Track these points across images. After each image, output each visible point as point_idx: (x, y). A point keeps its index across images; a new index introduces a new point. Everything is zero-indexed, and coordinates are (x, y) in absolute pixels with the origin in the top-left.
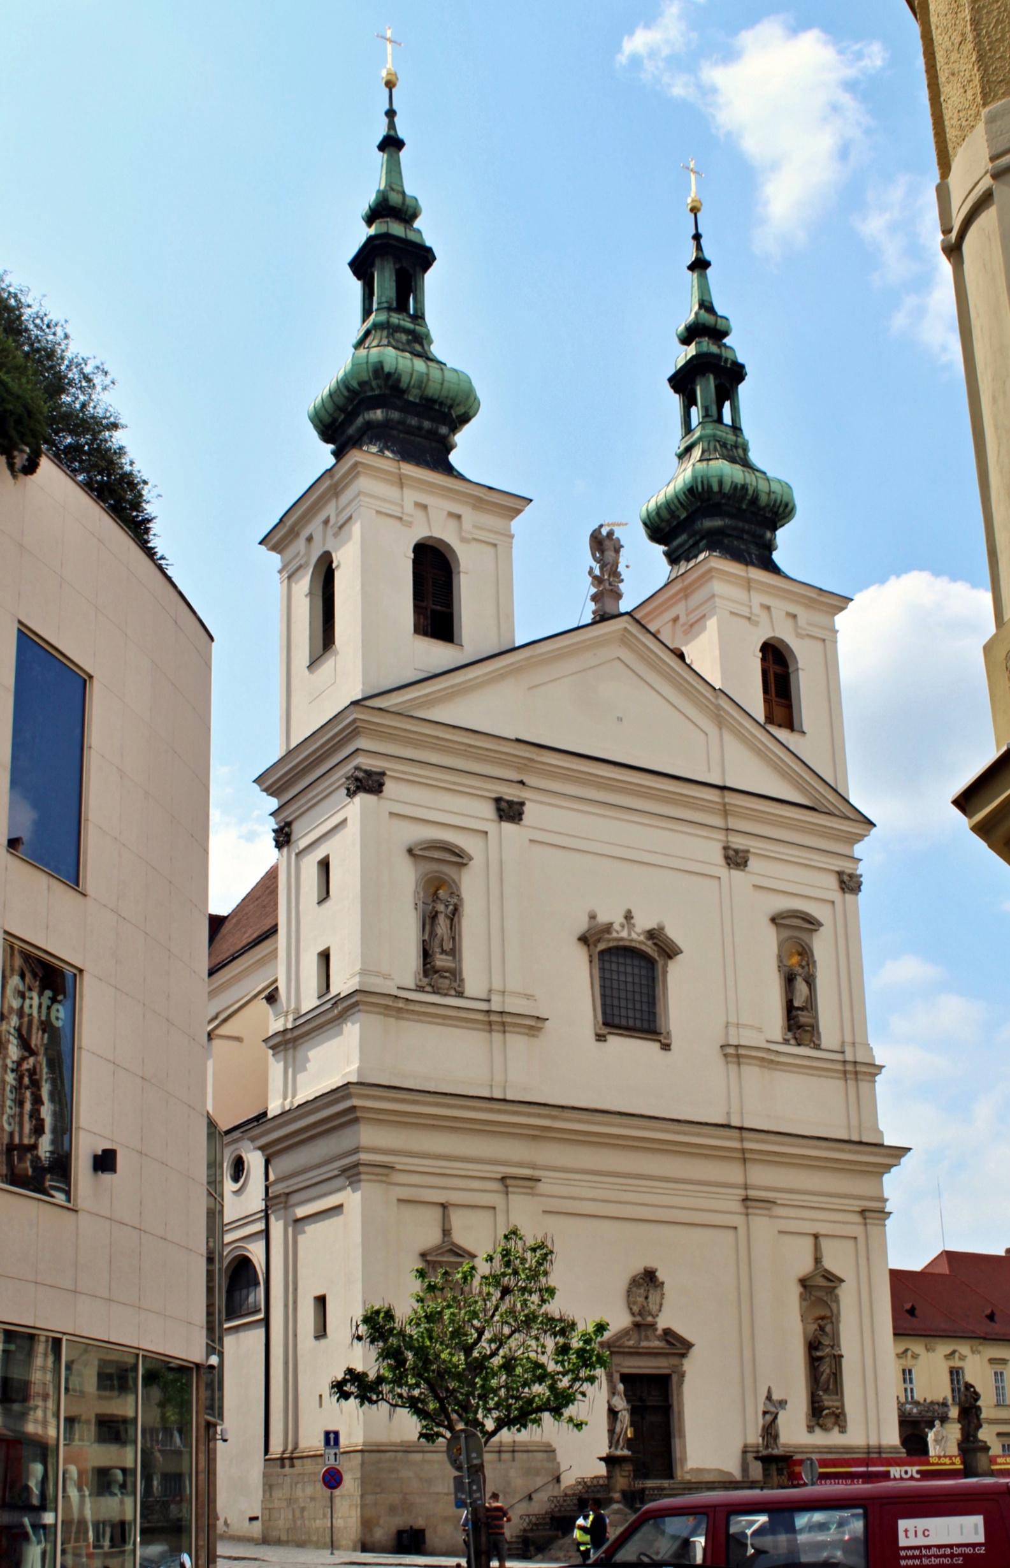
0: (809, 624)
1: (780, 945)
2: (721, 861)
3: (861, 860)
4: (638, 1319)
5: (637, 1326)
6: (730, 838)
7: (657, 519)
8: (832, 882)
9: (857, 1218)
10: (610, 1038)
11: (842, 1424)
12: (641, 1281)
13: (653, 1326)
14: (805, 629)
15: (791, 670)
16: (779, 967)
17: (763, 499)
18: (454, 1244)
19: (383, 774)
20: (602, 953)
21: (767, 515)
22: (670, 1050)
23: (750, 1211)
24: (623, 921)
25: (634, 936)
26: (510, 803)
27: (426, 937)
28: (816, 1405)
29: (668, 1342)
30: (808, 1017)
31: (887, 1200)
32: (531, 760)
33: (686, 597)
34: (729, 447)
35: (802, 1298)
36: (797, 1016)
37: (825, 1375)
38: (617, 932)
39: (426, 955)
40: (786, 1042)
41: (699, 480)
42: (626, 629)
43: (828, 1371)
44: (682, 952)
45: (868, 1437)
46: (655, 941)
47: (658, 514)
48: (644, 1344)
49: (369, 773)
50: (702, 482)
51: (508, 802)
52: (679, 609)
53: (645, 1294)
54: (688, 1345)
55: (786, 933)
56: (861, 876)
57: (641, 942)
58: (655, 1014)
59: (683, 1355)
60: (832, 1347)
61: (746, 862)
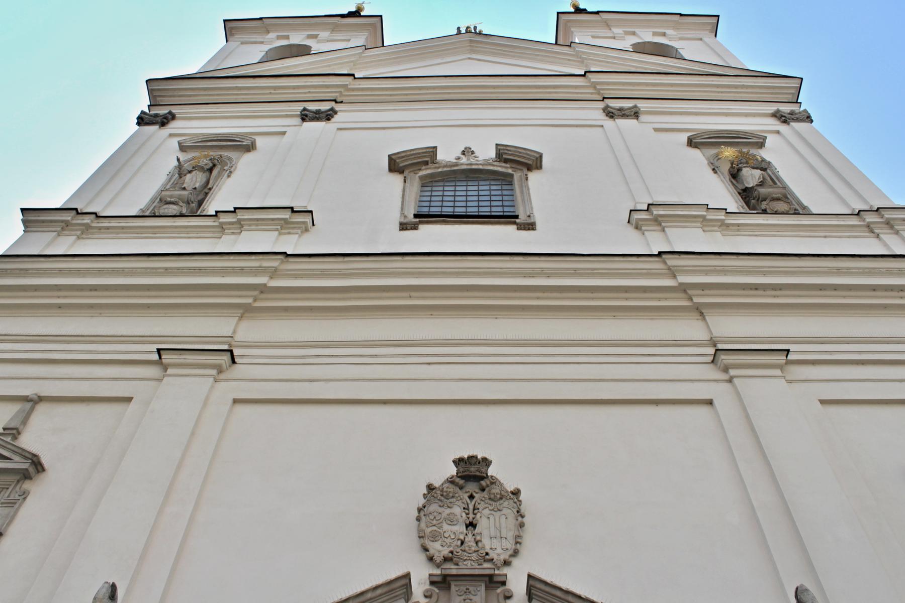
5: (442, 583)
13: (493, 582)
22: (534, 229)
23: (732, 372)
44: (541, 156)
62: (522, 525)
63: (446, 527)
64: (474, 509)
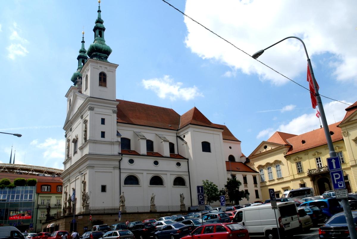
8: (111, 111)
9: (113, 169)
33: (88, 65)
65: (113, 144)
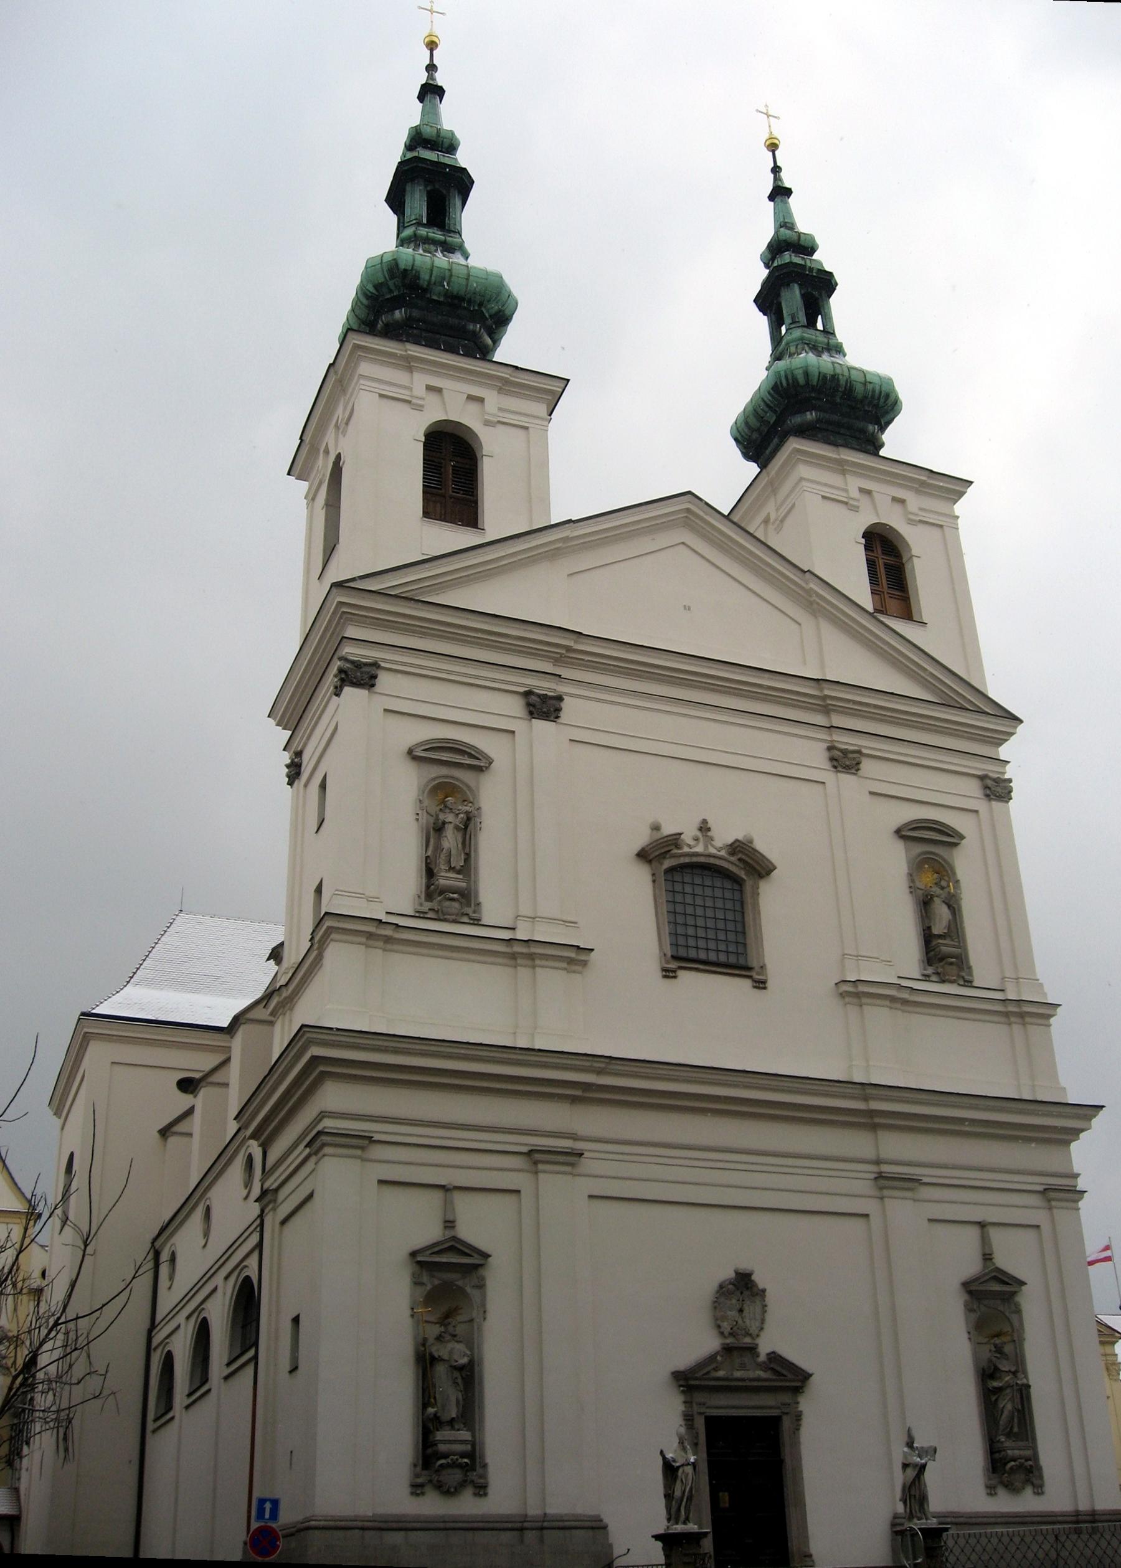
0: (921, 509)
1: (910, 862)
2: (827, 765)
3: (1009, 762)
4: (729, 1341)
5: (728, 1350)
6: (835, 737)
7: (746, 430)
8: (973, 788)
10: (680, 973)
11: (1036, 1482)
12: (731, 1287)
13: (752, 1350)
14: (917, 515)
15: (904, 560)
16: (910, 887)
17: (859, 389)
18: (454, 1238)
19: (375, 665)
20: (671, 870)
21: (867, 408)
22: (765, 988)
24: (699, 834)
25: (712, 851)
26: (544, 698)
27: (429, 853)
28: (997, 1456)
29: (772, 1369)
30: (954, 946)
31: (1077, 1176)
32: (569, 649)
34: (820, 349)
35: (969, 1309)
36: (938, 945)
37: (1006, 1413)
38: (689, 846)
39: (430, 872)
40: (926, 978)
41: (783, 374)
42: (688, 510)
43: (1009, 1407)
44: (775, 868)
45: (1075, 1497)
46: (740, 856)
47: (747, 423)
48: (738, 1374)
49: (358, 665)
50: (786, 377)
51: (539, 696)
52: (770, 509)
53: (738, 1307)
54: (805, 1376)
55: (919, 849)
56: (1010, 781)
57: (720, 858)
58: (745, 945)
59: (798, 1390)
60: (1015, 1373)
61: (858, 764)
62: (766, 1311)
63: (729, 1313)
64: (743, 1301)
65: (1022, 1015)
